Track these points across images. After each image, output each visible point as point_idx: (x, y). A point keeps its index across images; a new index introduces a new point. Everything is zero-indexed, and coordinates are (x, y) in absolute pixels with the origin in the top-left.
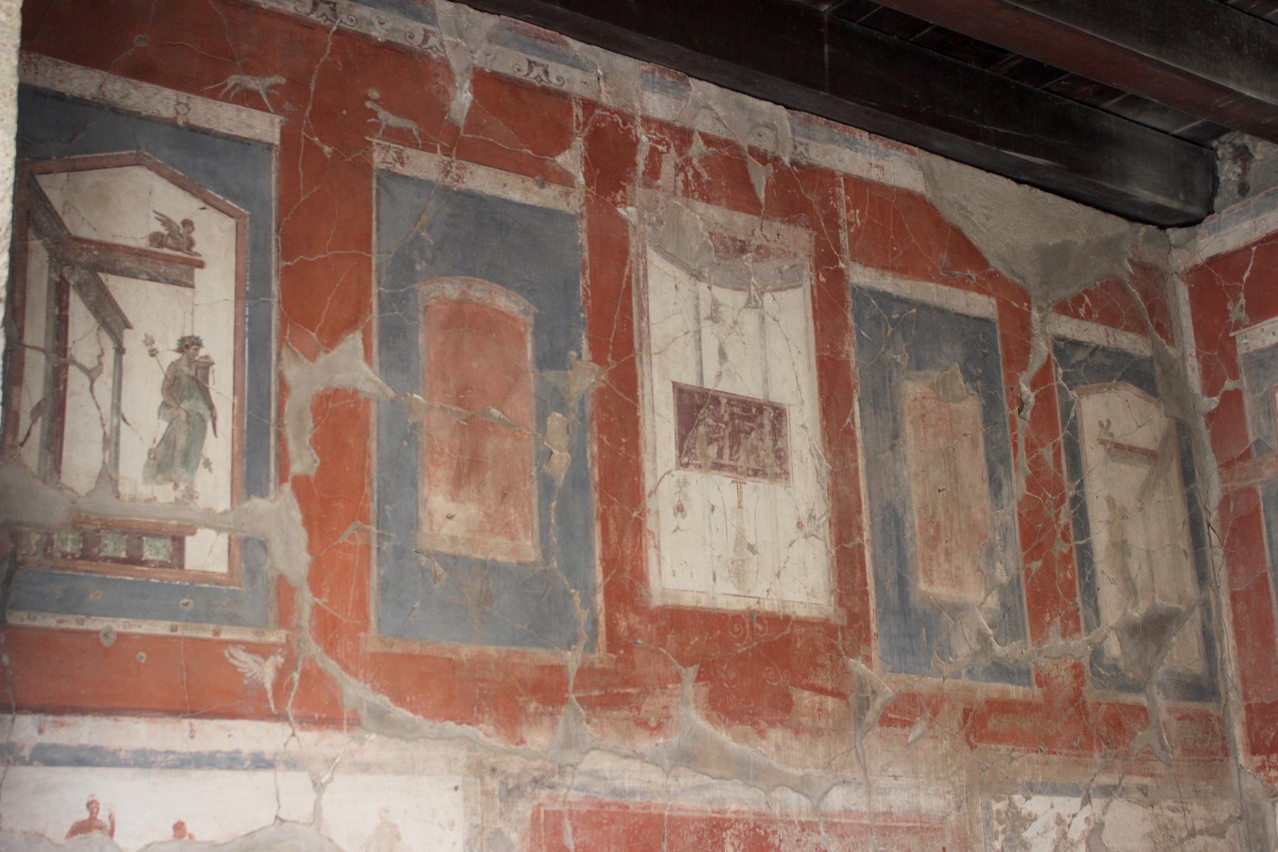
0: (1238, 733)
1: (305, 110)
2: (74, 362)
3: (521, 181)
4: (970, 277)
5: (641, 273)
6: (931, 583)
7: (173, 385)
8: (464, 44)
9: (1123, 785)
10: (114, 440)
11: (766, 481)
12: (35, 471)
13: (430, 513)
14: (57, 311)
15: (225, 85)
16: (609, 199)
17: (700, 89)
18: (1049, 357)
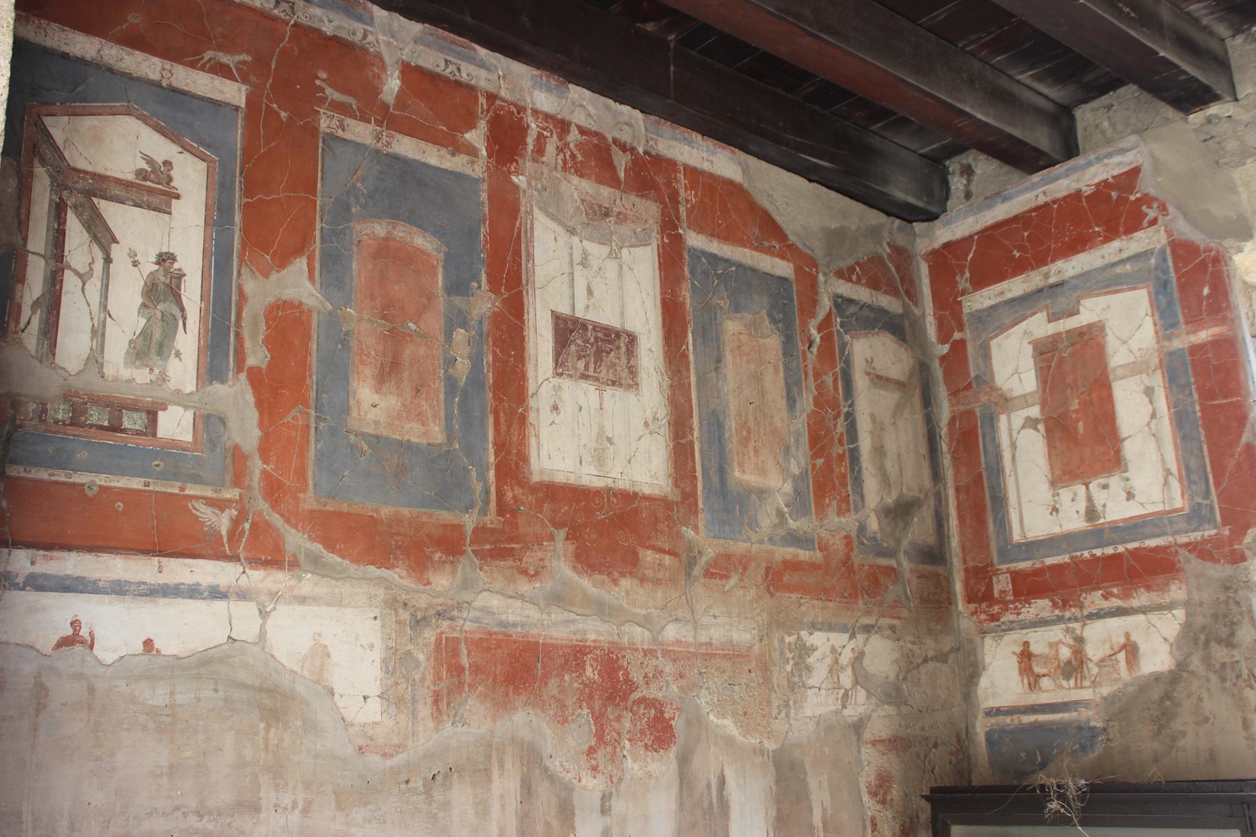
0: (959, 587)
2: (69, 267)
3: (436, 149)
4: (774, 247)
5: (529, 227)
6: (744, 472)
7: (152, 290)
8: (395, 43)
9: (879, 625)
10: (101, 331)
11: (622, 390)
12: (33, 352)
13: (358, 402)
14: (56, 226)
15: (203, 58)
16: (505, 169)
17: (577, 92)
18: (830, 309)
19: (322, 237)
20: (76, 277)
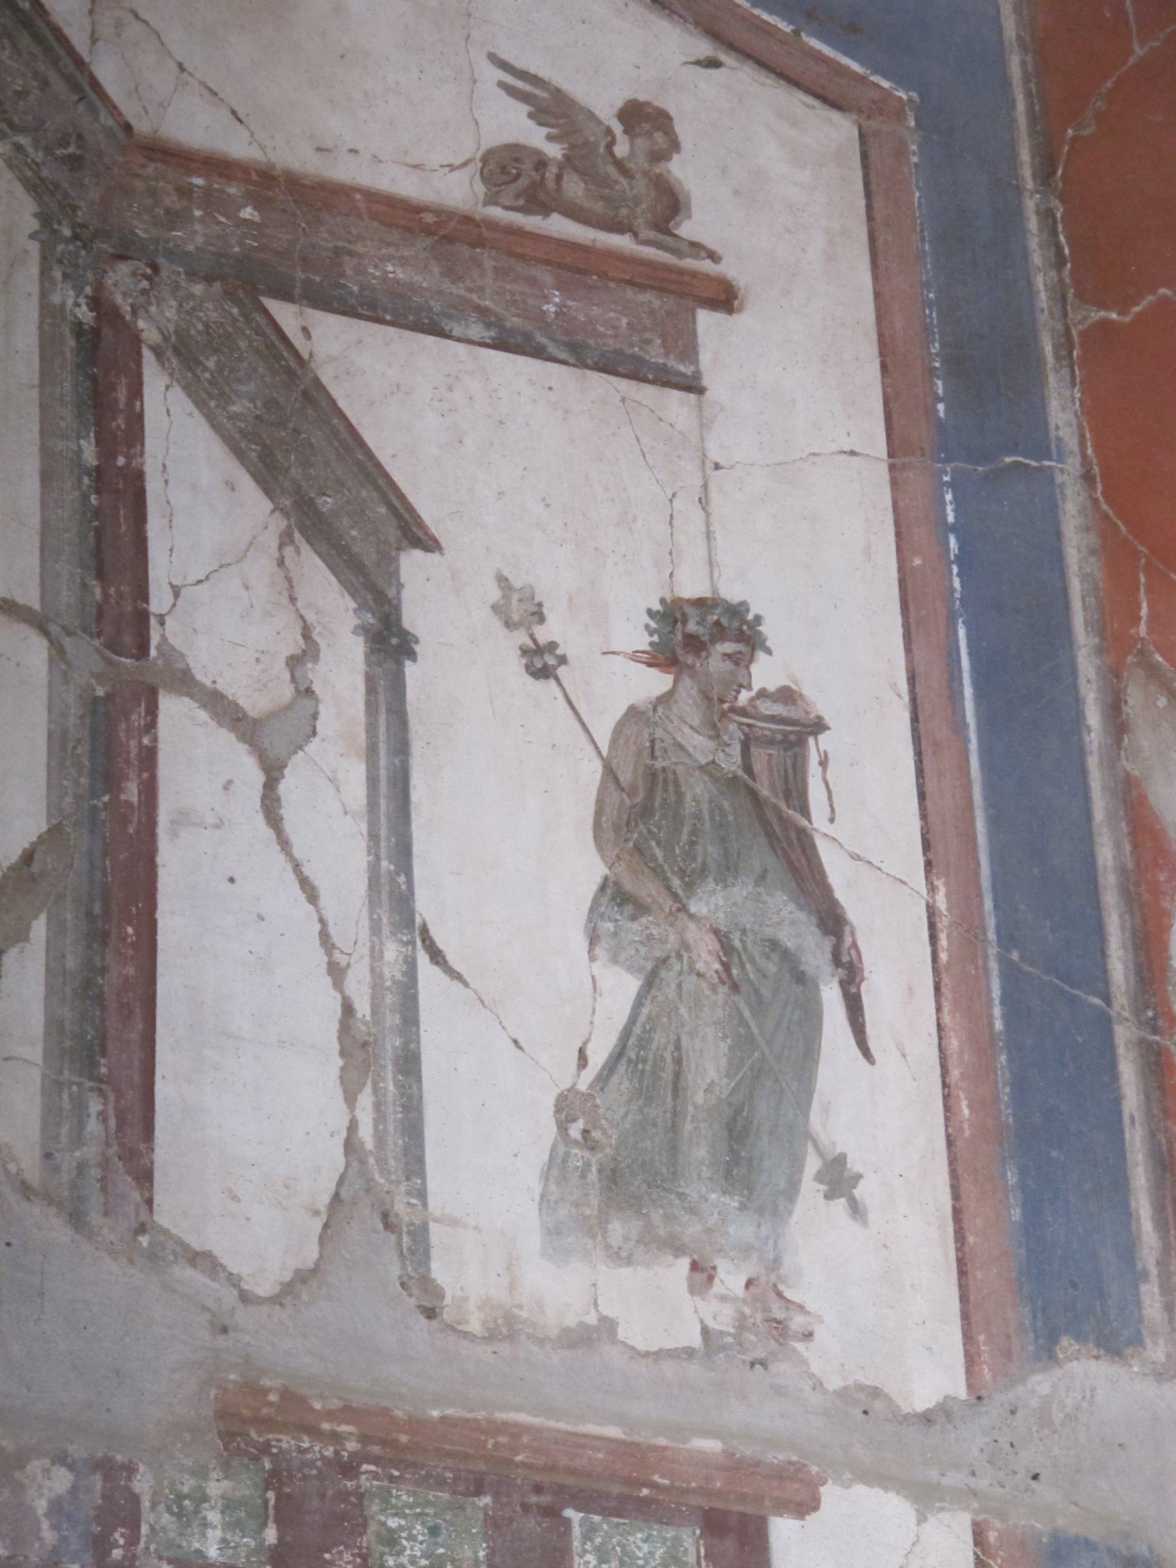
2: (185, 682)
7: (646, 811)
10: (392, 1044)
12: (29, 1164)
14: (89, 453)
20: (226, 738)
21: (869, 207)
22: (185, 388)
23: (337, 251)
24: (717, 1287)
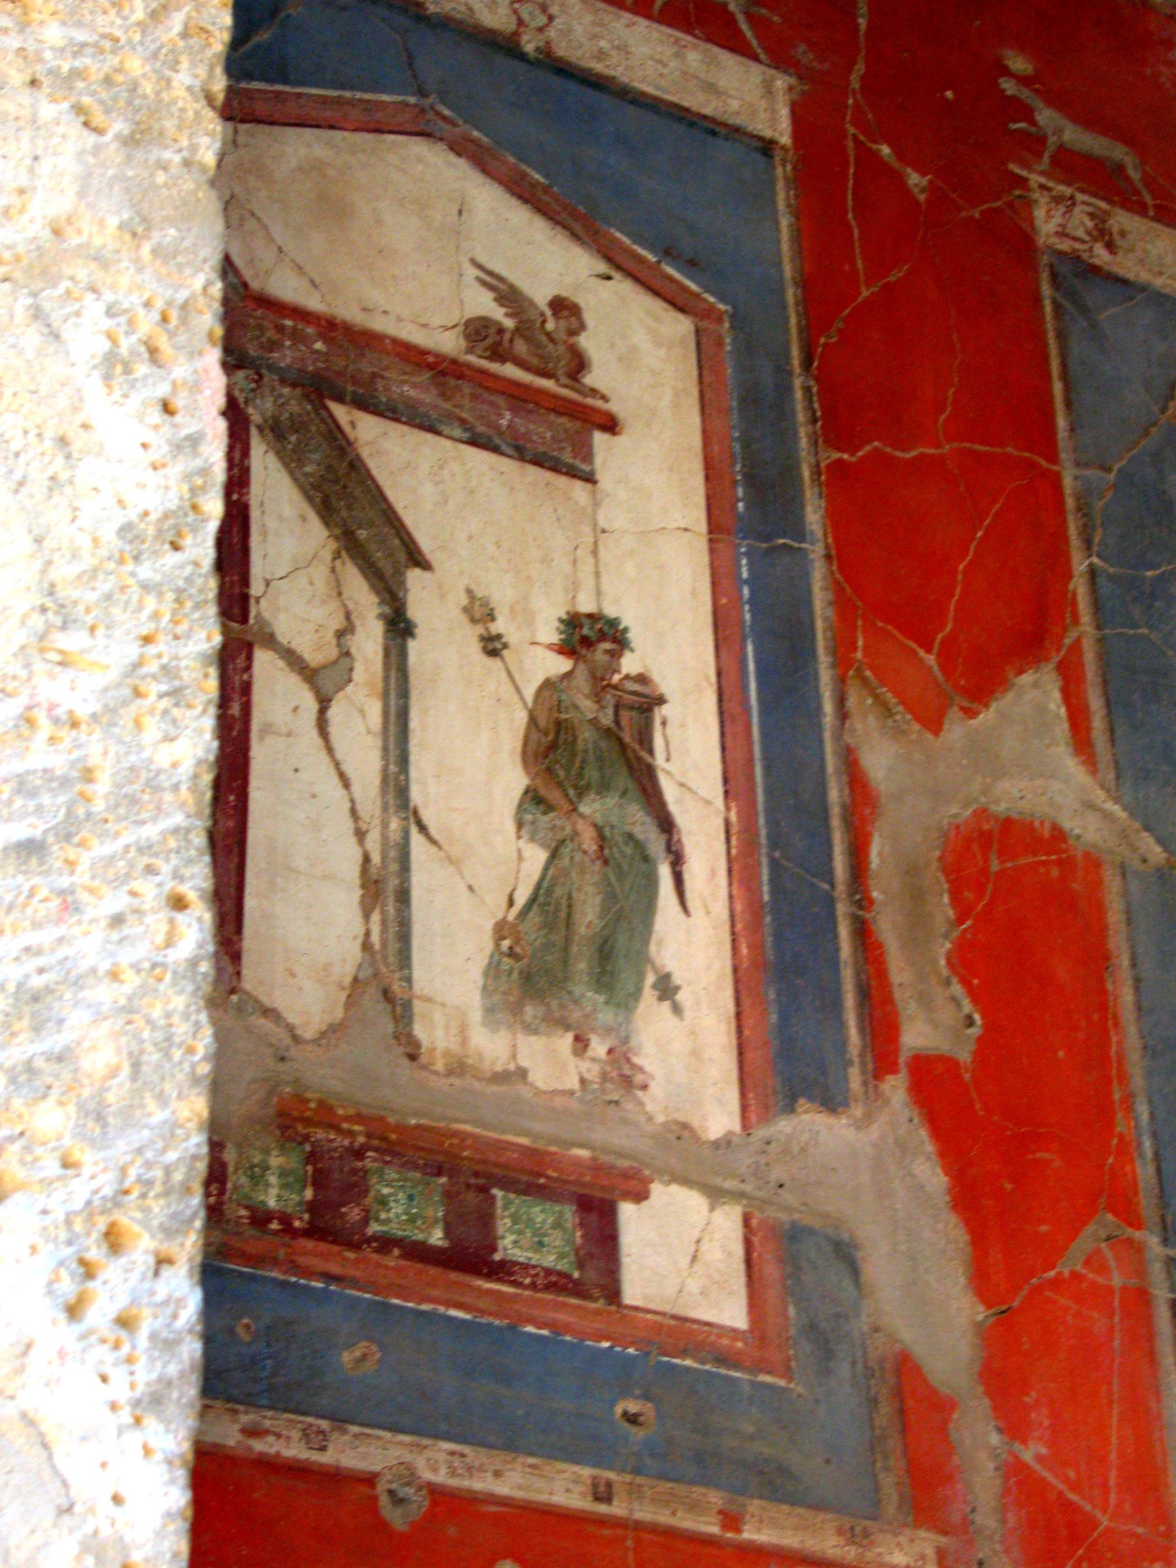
1: (849, 69)
2: (270, 641)
7: (553, 746)
10: (393, 883)
19: (1097, 605)
21: (700, 376)
22: (277, 453)
23: (374, 376)
24: (590, 1053)
